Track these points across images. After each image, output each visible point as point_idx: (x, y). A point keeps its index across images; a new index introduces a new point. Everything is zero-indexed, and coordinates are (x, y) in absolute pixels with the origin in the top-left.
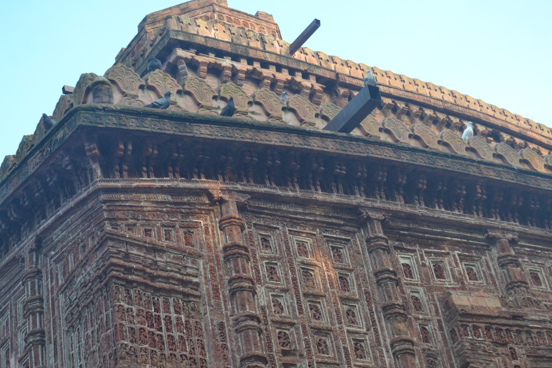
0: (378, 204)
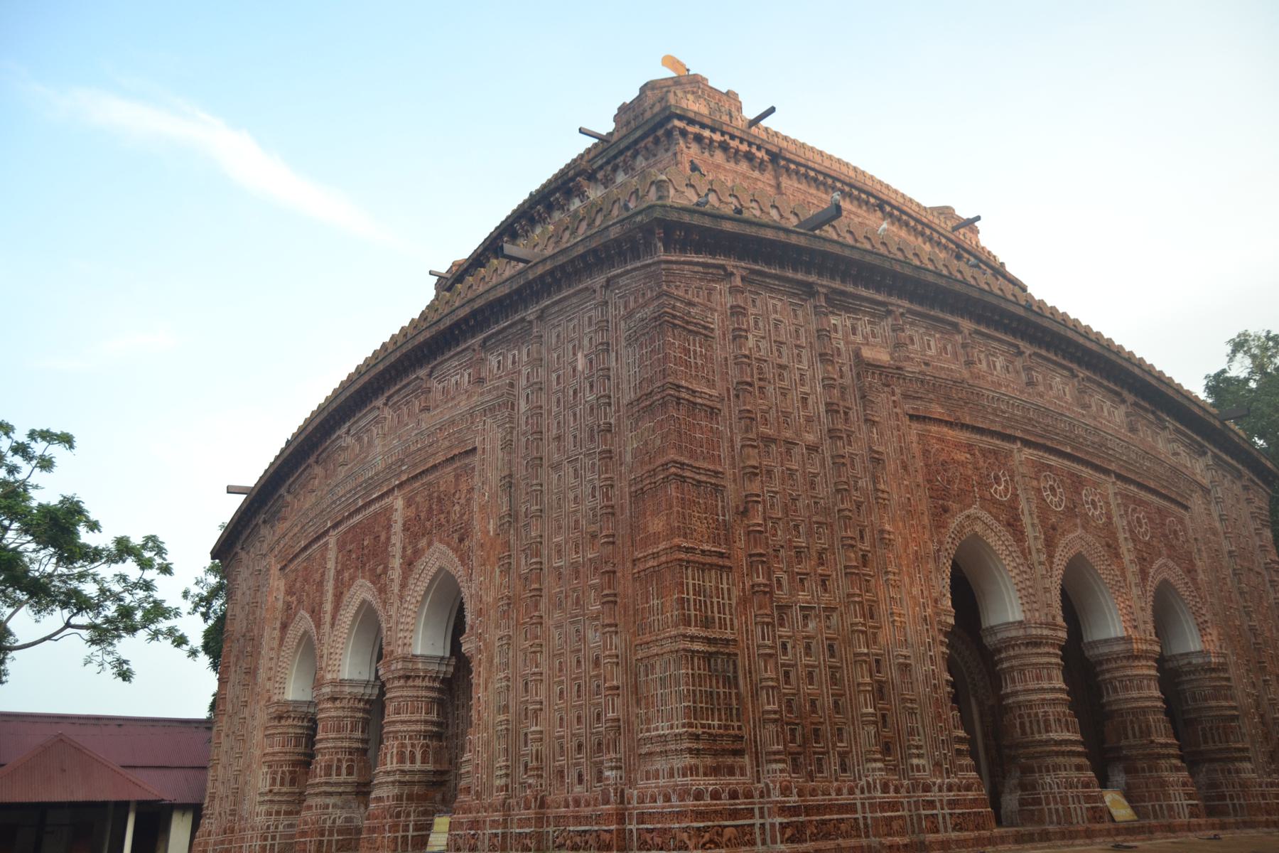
0: (824, 283)
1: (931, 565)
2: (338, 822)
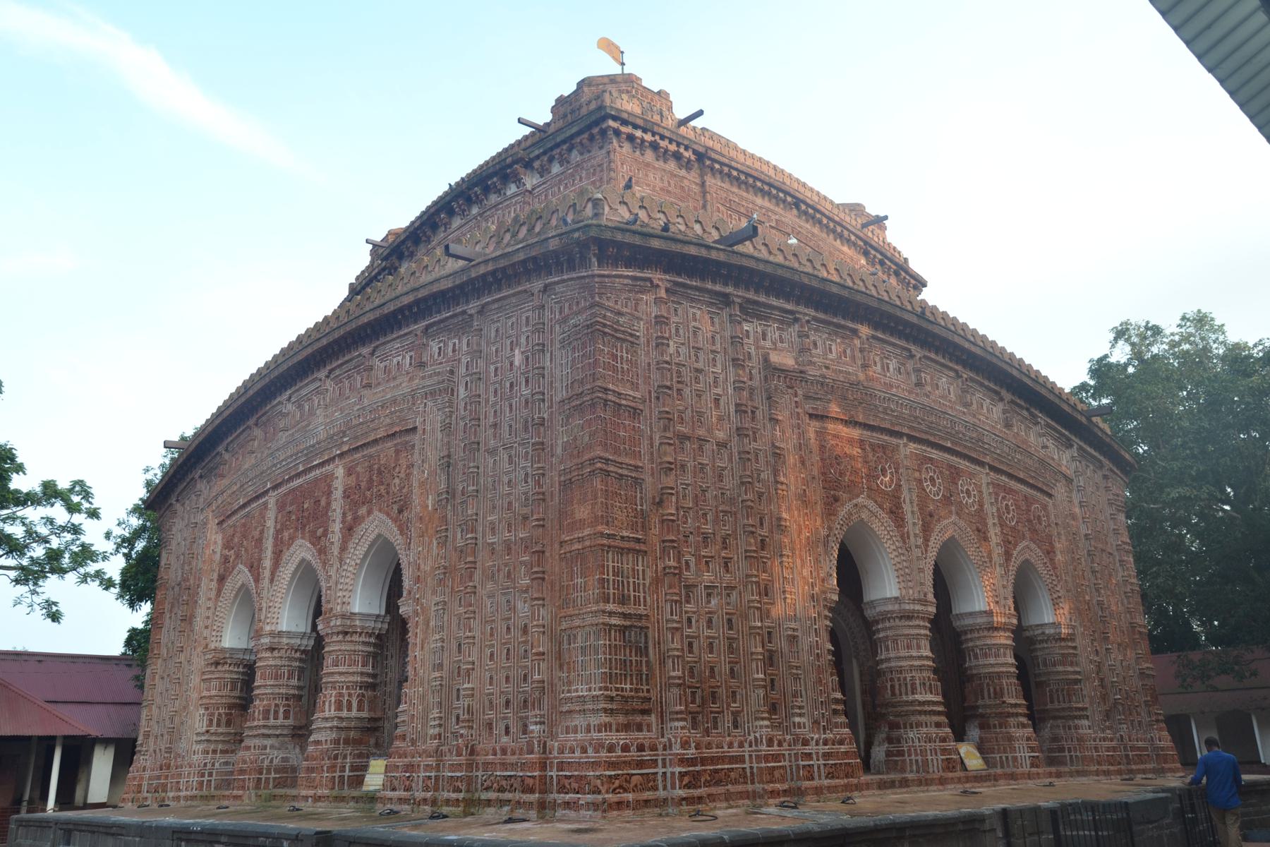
1: (821, 549)
2: (275, 762)
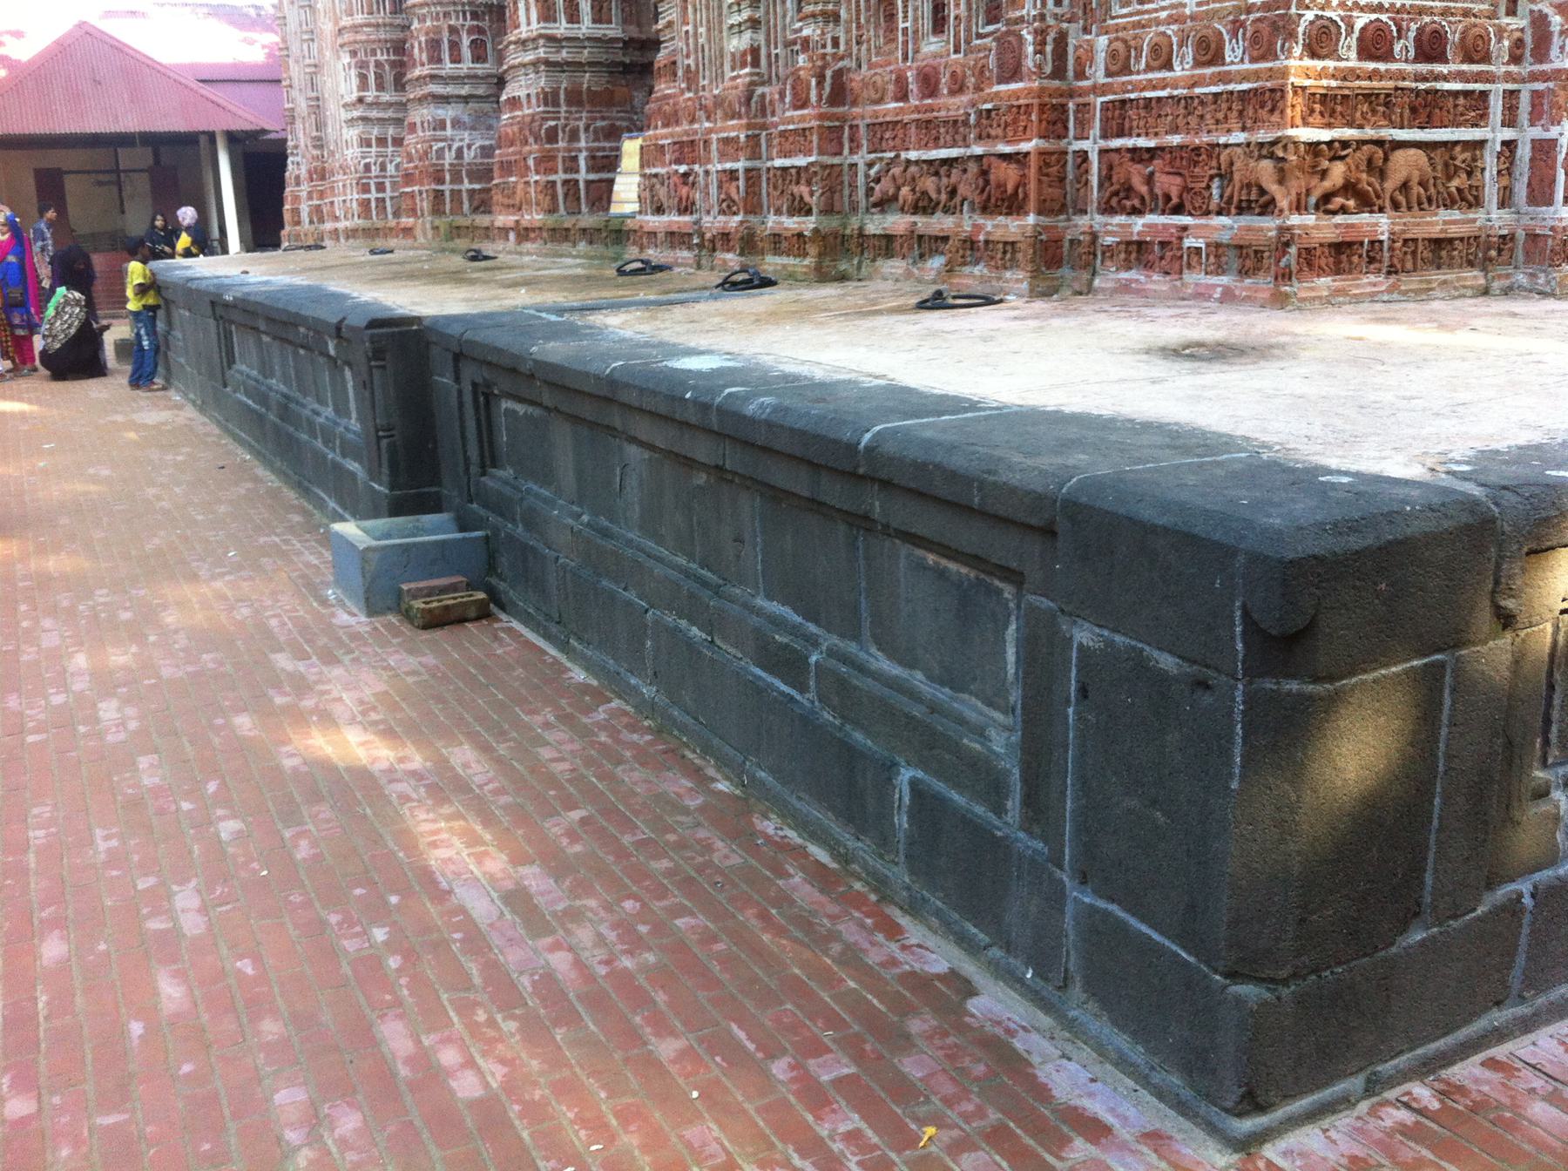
2: (468, 156)
